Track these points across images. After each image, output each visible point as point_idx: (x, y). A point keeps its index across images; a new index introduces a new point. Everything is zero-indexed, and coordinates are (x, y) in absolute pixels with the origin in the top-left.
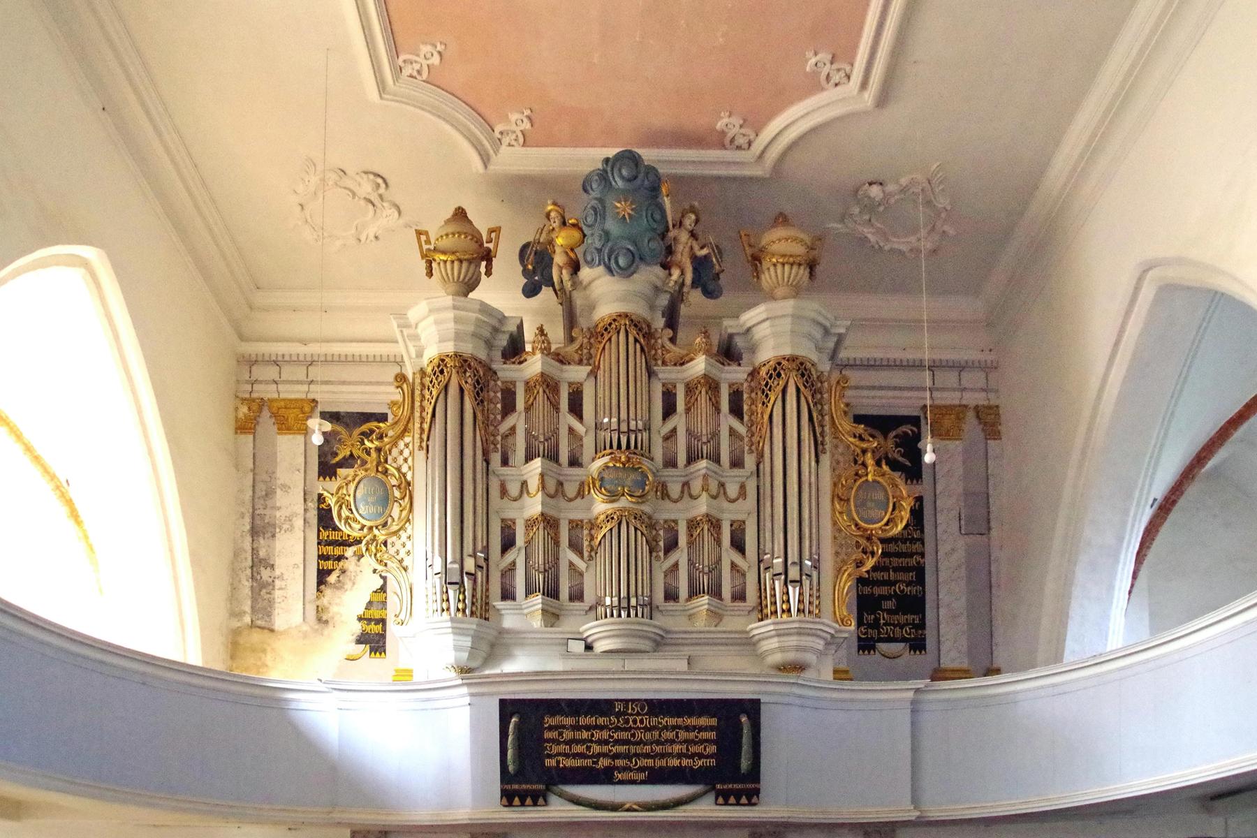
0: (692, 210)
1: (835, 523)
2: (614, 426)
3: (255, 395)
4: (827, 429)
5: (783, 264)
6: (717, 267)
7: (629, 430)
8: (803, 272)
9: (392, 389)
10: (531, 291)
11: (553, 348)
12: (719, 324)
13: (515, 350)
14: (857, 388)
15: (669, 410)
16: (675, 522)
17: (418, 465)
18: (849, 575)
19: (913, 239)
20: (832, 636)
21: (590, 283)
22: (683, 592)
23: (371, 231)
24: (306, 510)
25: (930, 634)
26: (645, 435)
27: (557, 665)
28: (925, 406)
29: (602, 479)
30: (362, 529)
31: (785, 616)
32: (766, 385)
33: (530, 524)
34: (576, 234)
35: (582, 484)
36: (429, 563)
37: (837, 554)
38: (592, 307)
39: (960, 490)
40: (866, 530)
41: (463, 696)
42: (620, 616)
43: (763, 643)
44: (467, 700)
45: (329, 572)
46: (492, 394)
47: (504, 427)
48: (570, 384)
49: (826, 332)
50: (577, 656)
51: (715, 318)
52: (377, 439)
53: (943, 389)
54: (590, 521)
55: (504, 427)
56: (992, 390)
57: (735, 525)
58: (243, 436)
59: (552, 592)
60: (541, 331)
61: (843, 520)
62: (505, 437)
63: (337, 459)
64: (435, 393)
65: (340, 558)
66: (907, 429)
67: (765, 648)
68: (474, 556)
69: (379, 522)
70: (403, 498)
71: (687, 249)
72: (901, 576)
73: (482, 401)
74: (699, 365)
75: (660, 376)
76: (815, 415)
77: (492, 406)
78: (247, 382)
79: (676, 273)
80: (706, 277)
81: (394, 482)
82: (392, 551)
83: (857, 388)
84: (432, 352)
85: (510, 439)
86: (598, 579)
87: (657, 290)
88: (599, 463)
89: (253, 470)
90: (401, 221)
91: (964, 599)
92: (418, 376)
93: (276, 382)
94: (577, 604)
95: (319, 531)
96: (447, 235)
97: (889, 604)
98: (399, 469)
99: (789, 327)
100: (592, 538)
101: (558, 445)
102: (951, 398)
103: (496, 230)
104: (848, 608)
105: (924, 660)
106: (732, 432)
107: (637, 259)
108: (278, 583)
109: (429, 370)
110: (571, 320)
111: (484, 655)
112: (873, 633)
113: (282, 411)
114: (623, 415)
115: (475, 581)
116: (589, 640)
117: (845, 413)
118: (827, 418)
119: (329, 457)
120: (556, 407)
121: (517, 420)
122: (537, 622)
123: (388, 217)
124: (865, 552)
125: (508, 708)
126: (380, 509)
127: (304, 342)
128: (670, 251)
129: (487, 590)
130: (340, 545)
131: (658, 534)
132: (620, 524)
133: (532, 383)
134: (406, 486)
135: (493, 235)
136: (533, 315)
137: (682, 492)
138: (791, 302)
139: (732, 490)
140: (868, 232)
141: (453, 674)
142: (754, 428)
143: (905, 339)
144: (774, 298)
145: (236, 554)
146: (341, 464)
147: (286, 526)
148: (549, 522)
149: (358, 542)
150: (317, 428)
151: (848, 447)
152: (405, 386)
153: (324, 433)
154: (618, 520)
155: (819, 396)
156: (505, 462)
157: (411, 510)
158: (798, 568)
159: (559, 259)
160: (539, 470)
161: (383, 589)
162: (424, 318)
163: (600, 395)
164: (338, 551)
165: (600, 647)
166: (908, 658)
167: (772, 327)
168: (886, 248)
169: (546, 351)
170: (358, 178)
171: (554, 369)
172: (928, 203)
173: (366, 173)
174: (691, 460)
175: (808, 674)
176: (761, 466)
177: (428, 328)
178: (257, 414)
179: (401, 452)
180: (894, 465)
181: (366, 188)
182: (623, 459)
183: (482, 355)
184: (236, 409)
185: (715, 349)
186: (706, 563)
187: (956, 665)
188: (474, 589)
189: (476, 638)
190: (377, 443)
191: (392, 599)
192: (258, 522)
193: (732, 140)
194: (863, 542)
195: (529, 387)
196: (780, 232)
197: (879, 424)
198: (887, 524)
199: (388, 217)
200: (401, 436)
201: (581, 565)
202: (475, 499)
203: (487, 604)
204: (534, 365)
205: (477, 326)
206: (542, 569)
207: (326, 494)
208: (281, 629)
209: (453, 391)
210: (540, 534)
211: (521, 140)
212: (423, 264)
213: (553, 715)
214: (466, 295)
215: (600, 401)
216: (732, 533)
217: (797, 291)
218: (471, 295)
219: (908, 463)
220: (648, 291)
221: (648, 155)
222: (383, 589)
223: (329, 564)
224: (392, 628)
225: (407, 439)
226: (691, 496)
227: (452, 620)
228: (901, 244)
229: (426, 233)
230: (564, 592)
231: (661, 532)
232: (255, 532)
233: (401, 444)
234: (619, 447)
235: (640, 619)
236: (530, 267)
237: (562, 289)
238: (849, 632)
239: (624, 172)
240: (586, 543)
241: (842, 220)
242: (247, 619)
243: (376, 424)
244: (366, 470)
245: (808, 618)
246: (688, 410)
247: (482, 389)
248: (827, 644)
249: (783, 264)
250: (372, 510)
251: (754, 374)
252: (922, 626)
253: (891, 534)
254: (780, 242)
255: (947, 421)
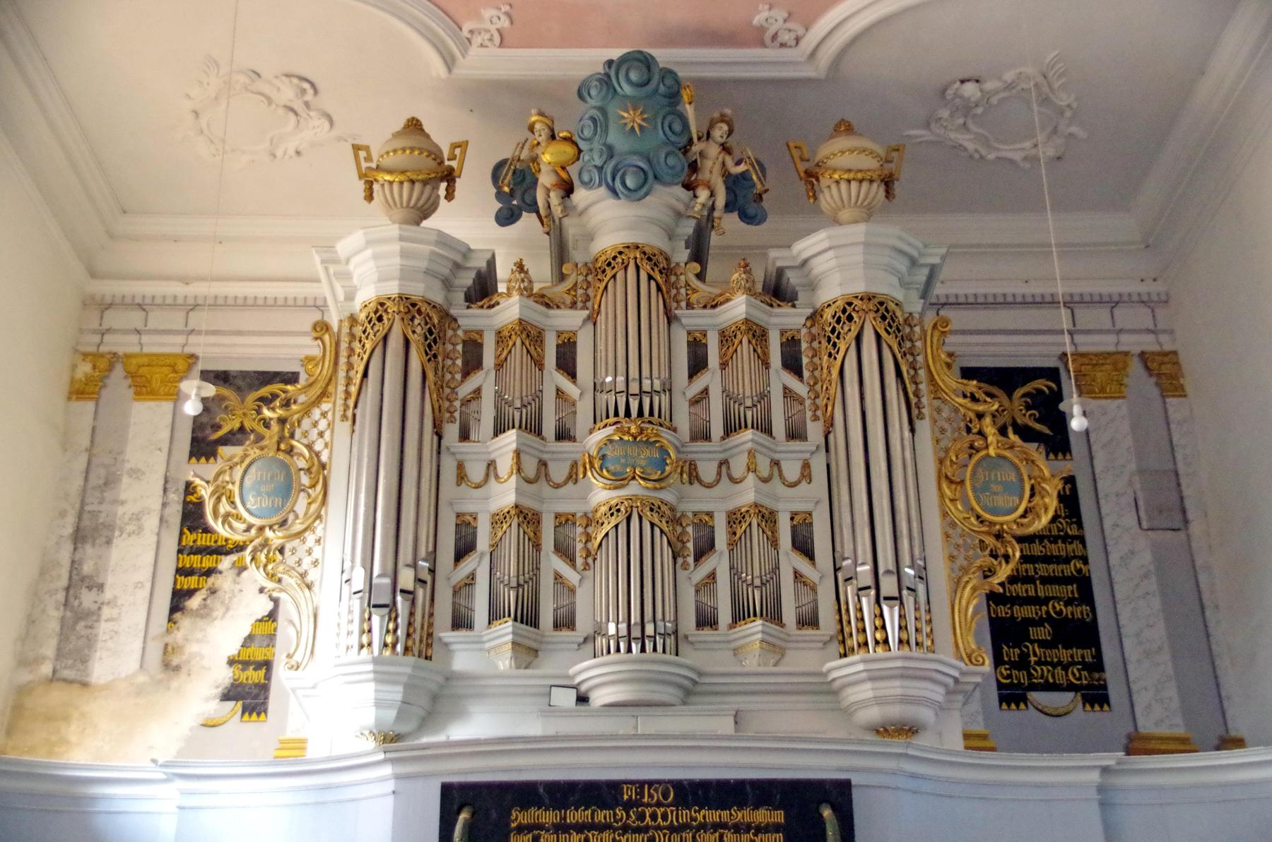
0: (723, 119)
1: (945, 514)
2: (621, 386)
3: (103, 349)
4: (923, 387)
5: (849, 181)
6: (759, 186)
7: (641, 391)
8: (878, 190)
9: (308, 340)
10: (507, 217)
11: (536, 289)
12: (765, 255)
13: (483, 290)
14: (964, 332)
15: (697, 365)
16: (710, 514)
17: (339, 442)
18: (974, 589)
19: (1027, 144)
20: (956, 680)
21: (586, 209)
22: (725, 616)
23: (291, 147)
24: (164, 505)
25: (1112, 676)
26: (665, 399)
27: (533, 727)
28: (1065, 354)
29: (603, 457)
30: (248, 530)
31: (879, 649)
32: (833, 331)
33: (498, 520)
34: (569, 150)
35: (574, 465)
36: (345, 577)
37: (952, 558)
38: (590, 237)
39: (1133, 466)
40: (994, 524)
41: (382, 779)
42: (629, 650)
43: (849, 691)
44: (390, 786)
45: (191, 593)
46: (449, 347)
47: (465, 390)
48: (559, 334)
49: (914, 263)
50: (564, 713)
51: (757, 247)
52: (282, 406)
53: (1088, 332)
54: (585, 514)
55: (465, 390)
56: (1164, 331)
57: (797, 518)
58: (82, 403)
59: (528, 617)
60: (520, 267)
61: (957, 511)
62: (466, 402)
63: (220, 433)
64: (368, 346)
65: (209, 572)
66: (1041, 384)
67: (853, 699)
68: (414, 566)
69: (274, 520)
70: (313, 486)
71: (717, 167)
72: (1054, 590)
73: (435, 356)
74: (738, 308)
75: (684, 321)
76: (904, 369)
77: (449, 362)
78: (95, 332)
79: (703, 195)
80: (744, 199)
81: (302, 464)
82: (291, 560)
83: (964, 332)
84: (367, 294)
85: (473, 405)
86: (597, 596)
87: (679, 215)
88: (600, 436)
89: (90, 450)
90: (335, 133)
91: (1161, 626)
92: (346, 325)
93: (138, 332)
94: (565, 633)
95: (182, 533)
96: (395, 151)
97: (1043, 633)
98: (309, 447)
99: (860, 258)
100: (589, 538)
101: (540, 409)
102: (1105, 343)
103: (463, 145)
104: (977, 635)
105: (1111, 721)
106: (787, 392)
107: (649, 178)
108: (106, 612)
109: (362, 316)
110: (561, 254)
111: (421, 713)
112: (1022, 676)
113: (143, 370)
114: (634, 373)
115: (413, 603)
116: (583, 688)
117: (949, 366)
118: (922, 372)
119: (208, 431)
120: (540, 364)
121: (485, 379)
122: (504, 662)
123: (315, 128)
124: (994, 555)
125: (454, 798)
126: (278, 501)
127: (186, 280)
128: (694, 167)
129: (431, 615)
130: (211, 553)
131: (684, 532)
132: (629, 519)
133: (506, 333)
134: (319, 469)
135: (458, 151)
136: (510, 248)
137: (719, 474)
138: (861, 228)
139: (792, 470)
140: (964, 139)
141: (370, 744)
142: (818, 387)
143: (1027, 274)
144: (836, 222)
145: (45, 570)
146: (225, 441)
147: (130, 528)
148: (527, 517)
149: (240, 548)
150: (193, 393)
151: (956, 410)
152: (327, 337)
153: (204, 400)
154: (627, 513)
155: (908, 344)
156: (465, 436)
157: (324, 501)
158: (895, 578)
159: (546, 179)
160: (514, 446)
161: (272, 616)
162: (360, 251)
163: (601, 347)
164: (208, 562)
165: (600, 697)
166: (1082, 715)
167: (837, 258)
168: (991, 157)
169: (527, 292)
170: (276, 82)
171: (537, 315)
172: (1045, 101)
173: (287, 76)
174: (730, 429)
175: (921, 740)
176: (831, 437)
177: (366, 263)
178: (102, 374)
179: (315, 424)
180: (1026, 434)
181: (287, 93)
182: (633, 430)
183: (438, 297)
184: (74, 367)
185: (759, 288)
186: (757, 573)
187: (1164, 730)
188: (412, 614)
189: (409, 687)
190: (280, 412)
191: (285, 631)
192: (86, 522)
193: (775, 37)
194: (990, 541)
195: (501, 338)
196: (843, 142)
197: (1002, 379)
198: (1023, 516)
199: (315, 128)
200: (317, 402)
201: (571, 576)
202: (419, 487)
203: (430, 635)
204: (509, 309)
205: (431, 260)
206: (514, 584)
207: (198, 481)
208: (102, 682)
209: (395, 343)
210: (512, 534)
211: (497, 39)
212: (360, 186)
213: (524, 807)
214: (418, 224)
215: (601, 355)
216: (794, 528)
217: (869, 213)
218: (425, 223)
219: (1046, 430)
220: (667, 218)
221: (663, 56)
222: (272, 616)
223: (192, 582)
224: (281, 673)
225: (326, 406)
226: (731, 479)
227: (375, 661)
228: (1014, 152)
229: (367, 148)
230: (547, 618)
231: (690, 529)
232: (79, 537)
233: (316, 413)
234: (628, 413)
235: (659, 655)
236: (506, 189)
237: (550, 214)
238: (982, 674)
239: (634, 76)
240: (579, 546)
241: (927, 126)
242: (46, 669)
243: (281, 386)
244: (262, 449)
245: (916, 653)
246: (724, 365)
247: (435, 341)
248: (949, 692)
249: (849, 181)
250: (266, 503)
251: (814, 317)
252: (1097, 665)
253: (1031, 530)
254: (842, 154)
255: (1101, 374)
